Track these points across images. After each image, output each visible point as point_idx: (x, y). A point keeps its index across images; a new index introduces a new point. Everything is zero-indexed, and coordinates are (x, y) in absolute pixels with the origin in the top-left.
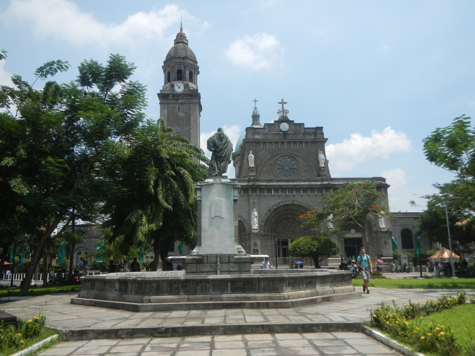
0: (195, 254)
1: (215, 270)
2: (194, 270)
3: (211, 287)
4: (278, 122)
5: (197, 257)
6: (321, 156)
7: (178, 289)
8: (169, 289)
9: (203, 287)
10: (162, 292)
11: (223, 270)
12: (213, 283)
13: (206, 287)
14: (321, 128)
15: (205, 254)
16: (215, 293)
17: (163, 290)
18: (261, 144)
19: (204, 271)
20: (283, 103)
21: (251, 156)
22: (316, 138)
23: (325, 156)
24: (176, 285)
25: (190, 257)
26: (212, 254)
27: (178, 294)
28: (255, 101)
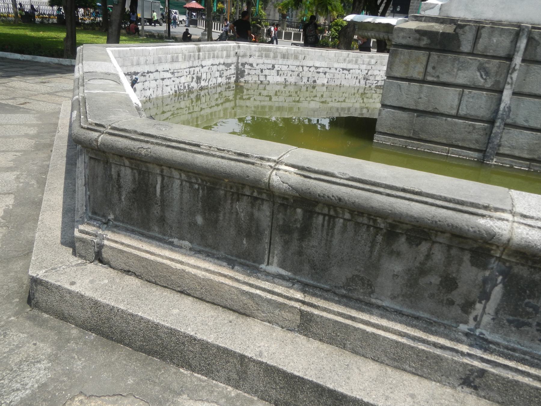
0: (434, 13)
1: (497, 82)
2: (417, 72)
3: (497, 292)
5: (438, 28)
7: (252, 231)
8: (199, 220)
9: (423, 272)
10: (162, 220)
11: (526, 90)
12: (522, 271)
13: (449, 283)
15: (470, 17)
16: (513, 340)
17: (172, 216)
19: (451, 80)
24: (242, 207)
25: (413, 25)
26: (500, 23)
27: (246, 259)
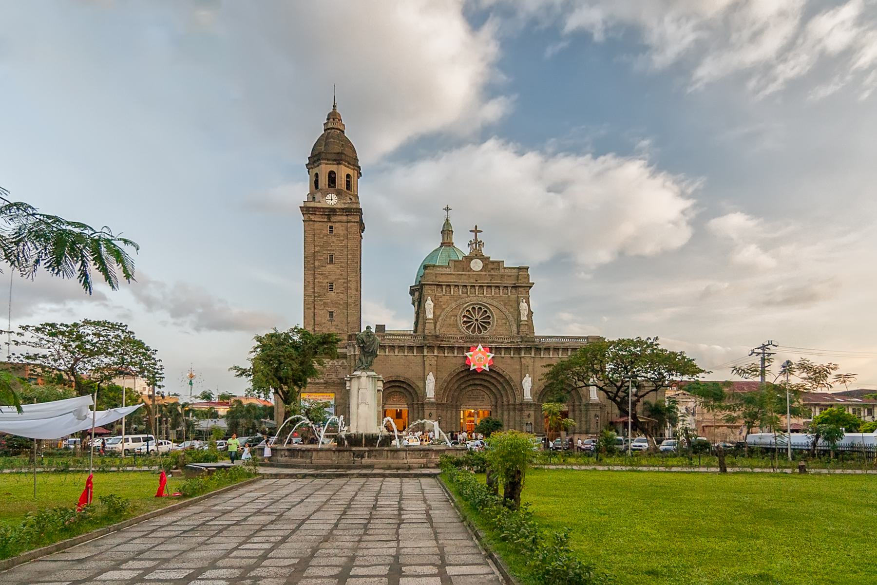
4: (469, 259)
6: (523, 305)
14: (527, 268)
18: (444, 287)
20: (476, 231)
21: (429, 305)
22: (519, 283)
23: (529, 305)
28: (447, 209)
